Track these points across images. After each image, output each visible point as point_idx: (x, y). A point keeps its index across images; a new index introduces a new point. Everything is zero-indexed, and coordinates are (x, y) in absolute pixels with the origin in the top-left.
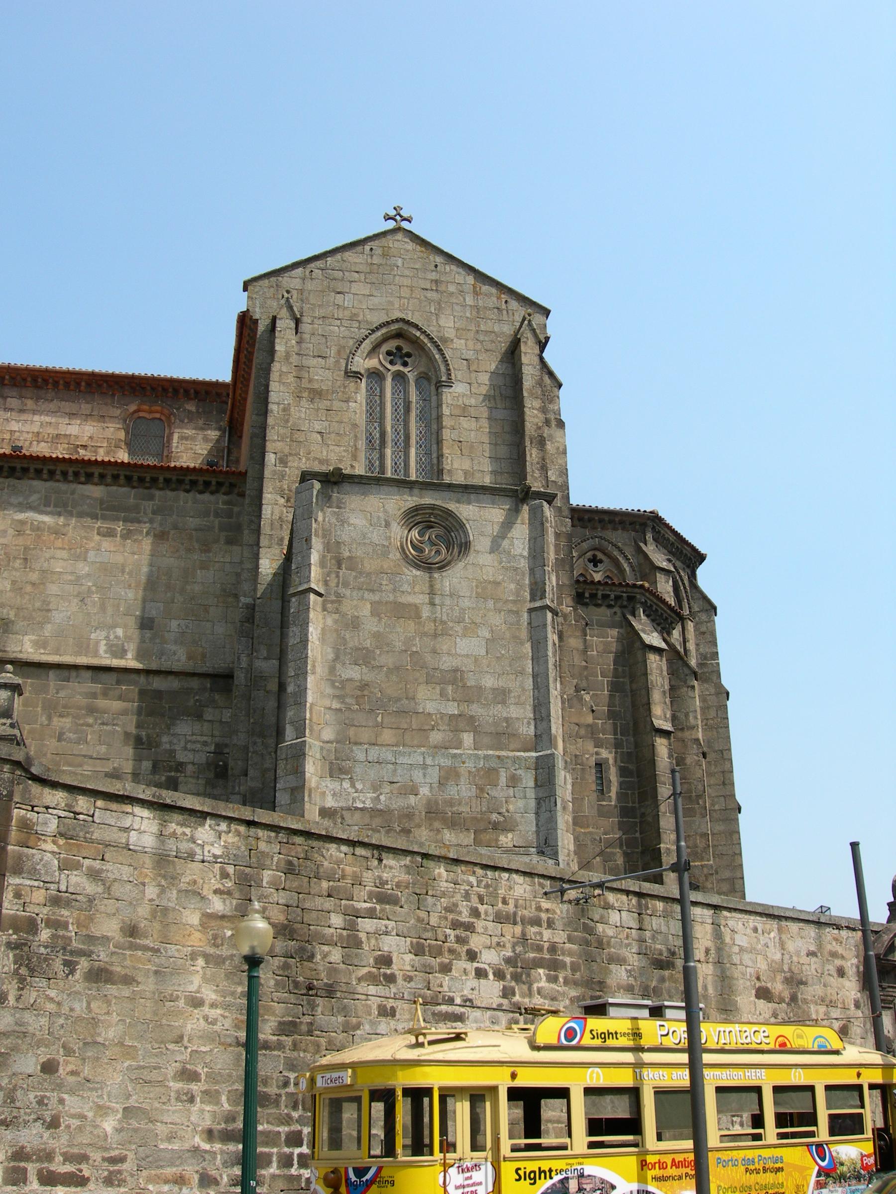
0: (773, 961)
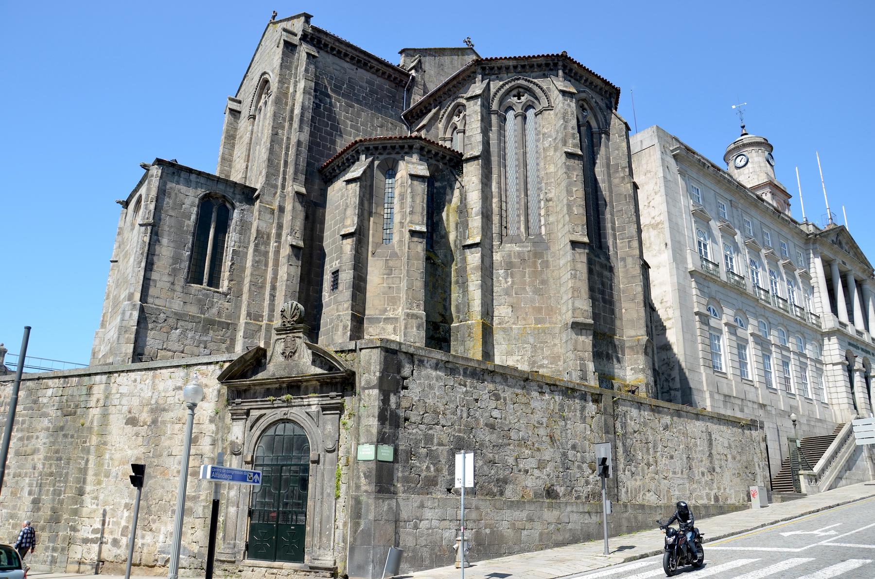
0: (143, 398)
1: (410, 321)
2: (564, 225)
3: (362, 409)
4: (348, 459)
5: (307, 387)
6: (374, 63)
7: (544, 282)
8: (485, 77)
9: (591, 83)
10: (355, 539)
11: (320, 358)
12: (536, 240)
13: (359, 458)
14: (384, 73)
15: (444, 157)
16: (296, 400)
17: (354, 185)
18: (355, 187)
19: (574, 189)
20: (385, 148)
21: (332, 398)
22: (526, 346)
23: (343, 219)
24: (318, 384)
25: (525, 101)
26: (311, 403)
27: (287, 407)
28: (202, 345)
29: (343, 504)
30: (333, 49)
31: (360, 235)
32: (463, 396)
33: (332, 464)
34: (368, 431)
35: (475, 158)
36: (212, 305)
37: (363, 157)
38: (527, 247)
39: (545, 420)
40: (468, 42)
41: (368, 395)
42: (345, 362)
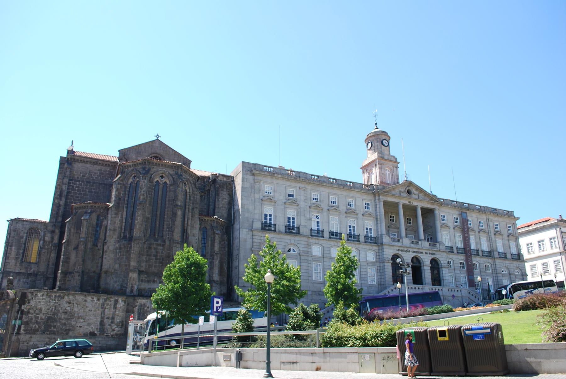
6: (100, 162)
19: (139, 218)
28: (26, 283)
30: (81, 161)
36: (31, 269)
39: (93, 309)
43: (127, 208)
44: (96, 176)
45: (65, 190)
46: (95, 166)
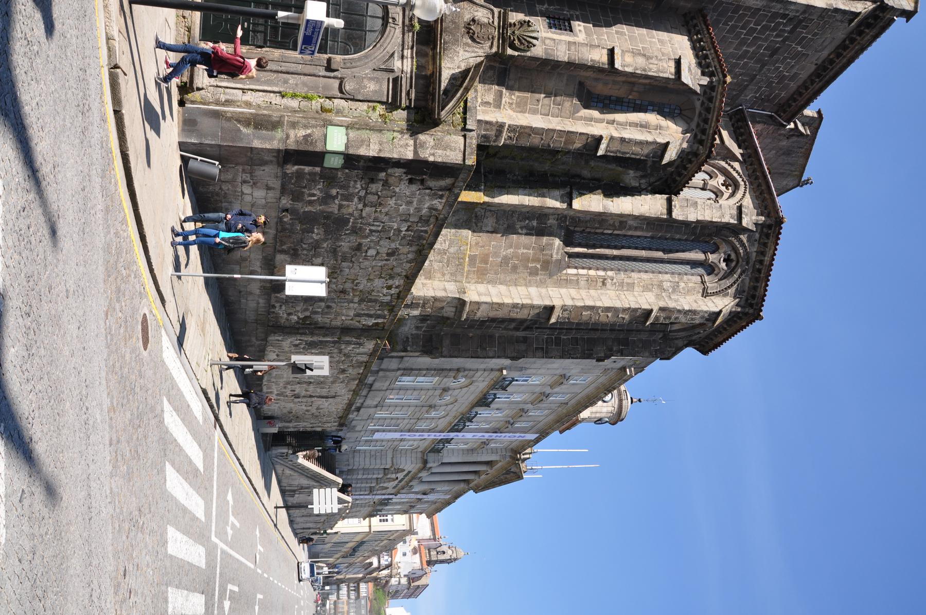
1: (494, 128)
2: (573, 299)
3: (389, 135)
4: (330, 111)
5: (426, 55)
6: (817, 86)
7: (515, 268)
8: (759, 227)
9: (720, 333)
10: (229, 119)
11: (460, 80)
12: (563, 263)
13: (330, 128)
14: (801, 94)
15: (680, 175)
16: (410, 39)
17: (673, 70)
18: (668, 71)
19: (610, 315)
20: (708, 110)
21: (408, 94)
22: (447, 243)
23: (635, 53)
24: (429, 73)
25: (720, 266)
26: (405, 61)
27: (403, 22)
29: (273, 102)
31: (609, 72)
32: (395, 228)
33: (326, 88)
34: (363, 141)
35: (670, 210)
37: (705, 81)
38: (557, 253)
40: (807, 182)
41: (407, 144)
42: (449, 113)
43: (652, 237)
44: (781, 69)
45: (787, 9)
46: (813, 67)
